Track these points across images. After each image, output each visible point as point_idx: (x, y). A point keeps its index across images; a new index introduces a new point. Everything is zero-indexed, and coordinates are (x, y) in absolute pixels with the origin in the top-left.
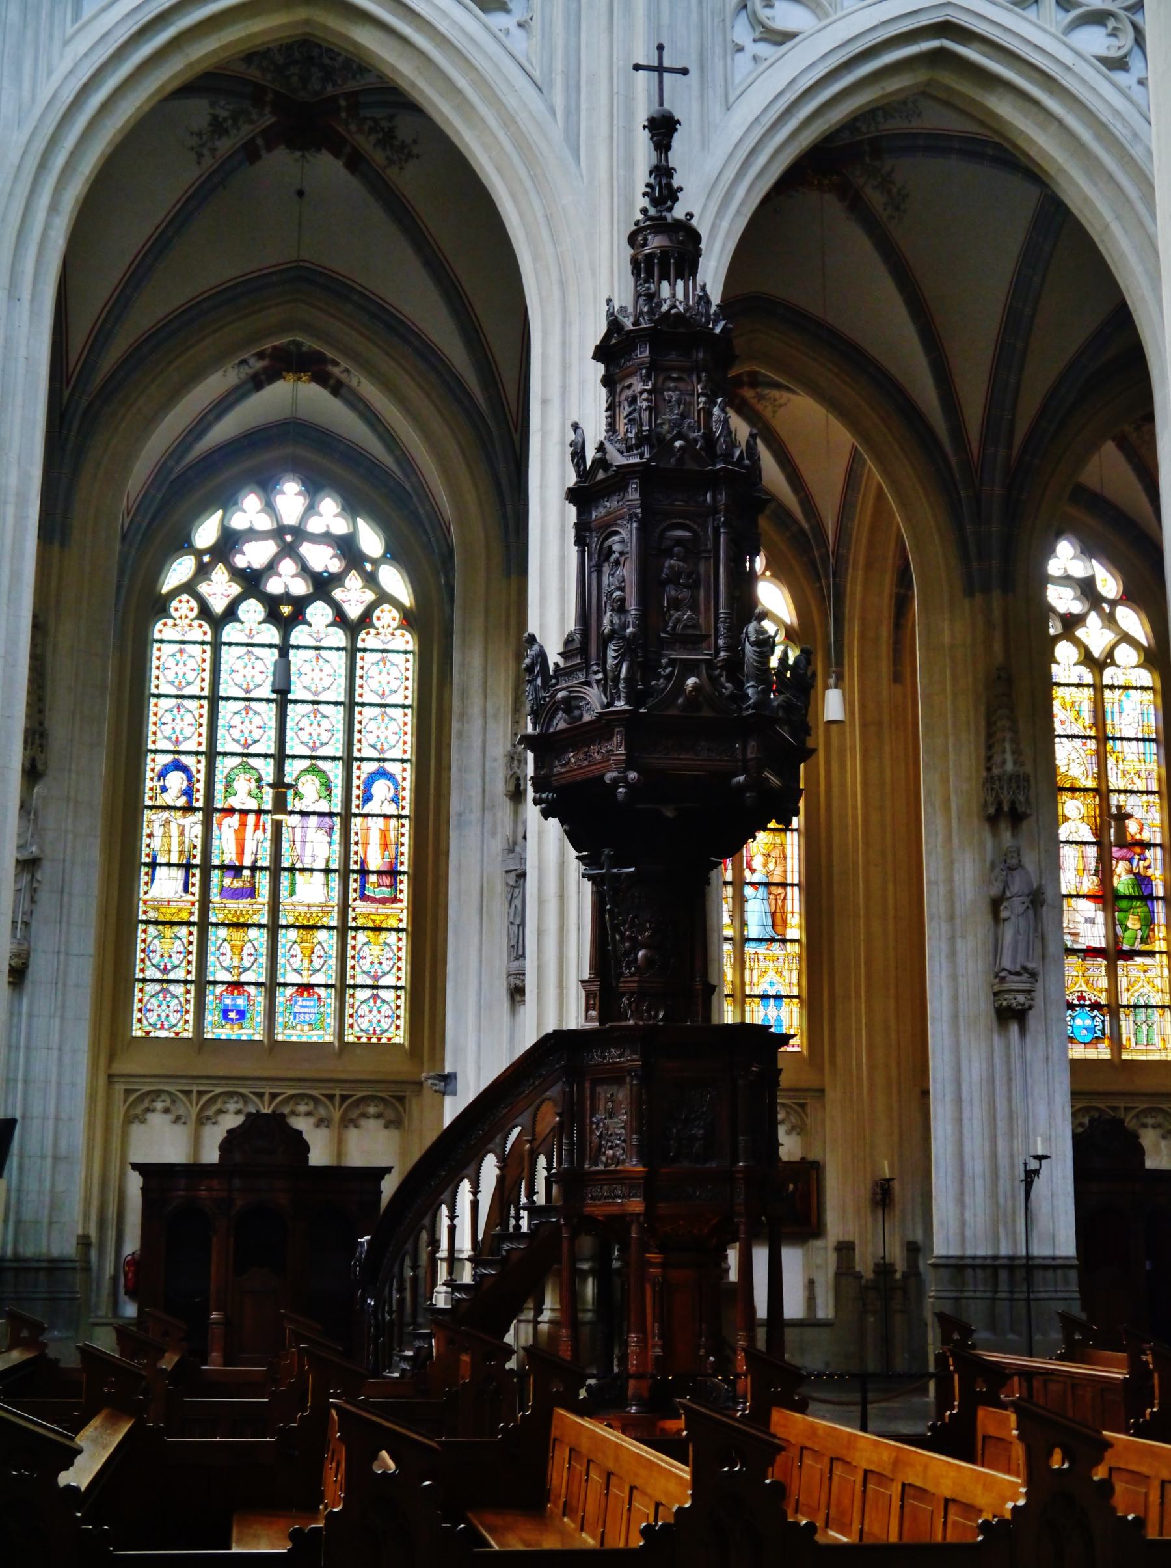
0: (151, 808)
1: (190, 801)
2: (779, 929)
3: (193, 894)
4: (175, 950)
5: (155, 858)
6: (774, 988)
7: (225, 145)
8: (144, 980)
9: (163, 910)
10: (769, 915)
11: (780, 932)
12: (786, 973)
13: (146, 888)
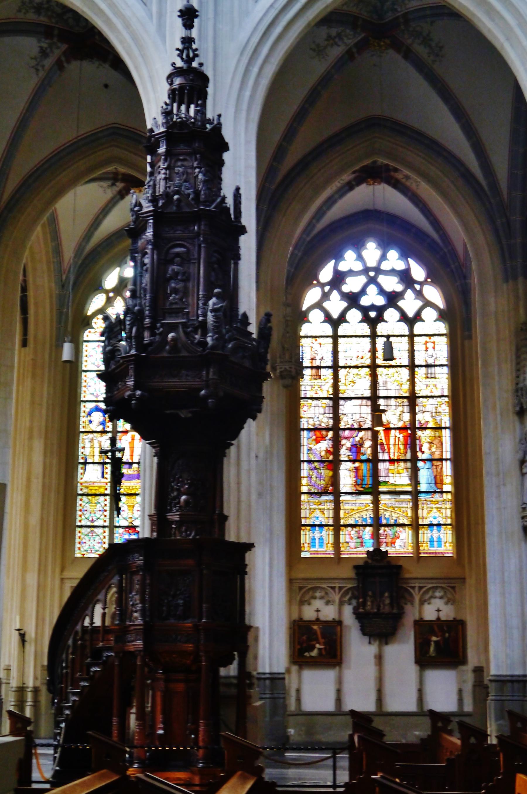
1: (104, 428)
2: (439, 485)
3: (106, 478)
4: (97, 509)
5: (86, 460)
6: (436, 519)
7: (48, 62)
8: (81, 527)
9: (91, 488)
10: (433, 478)
11: (440, 487)
12: (443, 511)
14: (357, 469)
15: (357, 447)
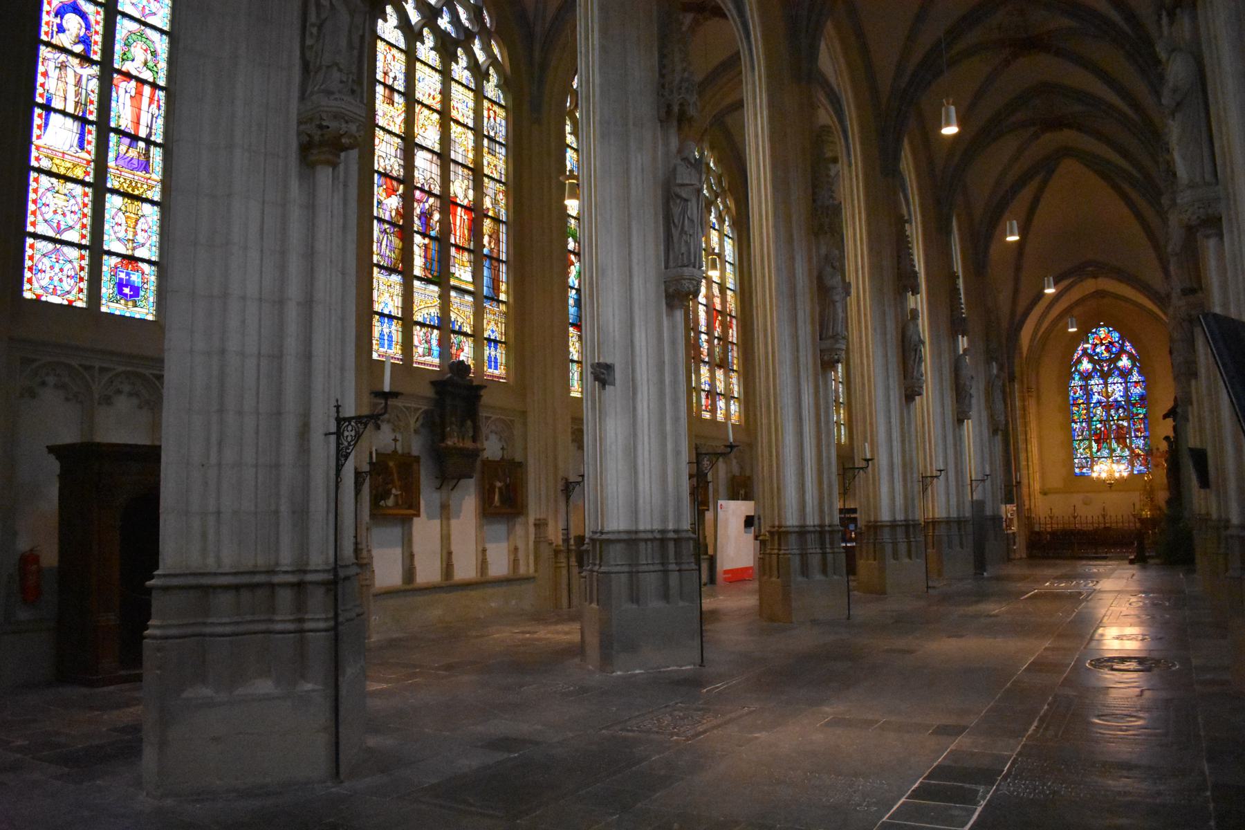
0: (48, 44)
4: (69, 208)
12: (499, 325)
14: (425, 245)
15: (426, 216)
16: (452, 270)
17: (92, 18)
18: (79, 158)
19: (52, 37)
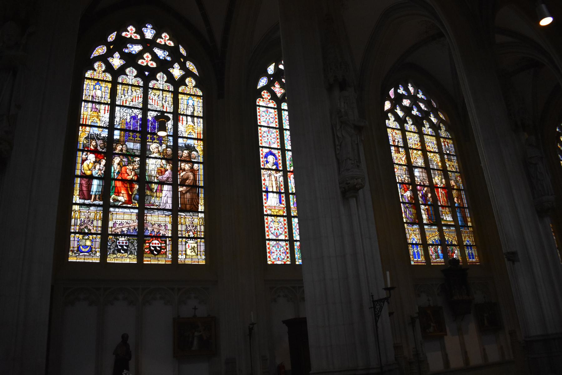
0: (264, 169)
12: (471, 237)
13: (265, 201)
15: (424, 196)
16: (442, 217)
17: (277, 155)
18: (280, 207)
19: (265, 166)
